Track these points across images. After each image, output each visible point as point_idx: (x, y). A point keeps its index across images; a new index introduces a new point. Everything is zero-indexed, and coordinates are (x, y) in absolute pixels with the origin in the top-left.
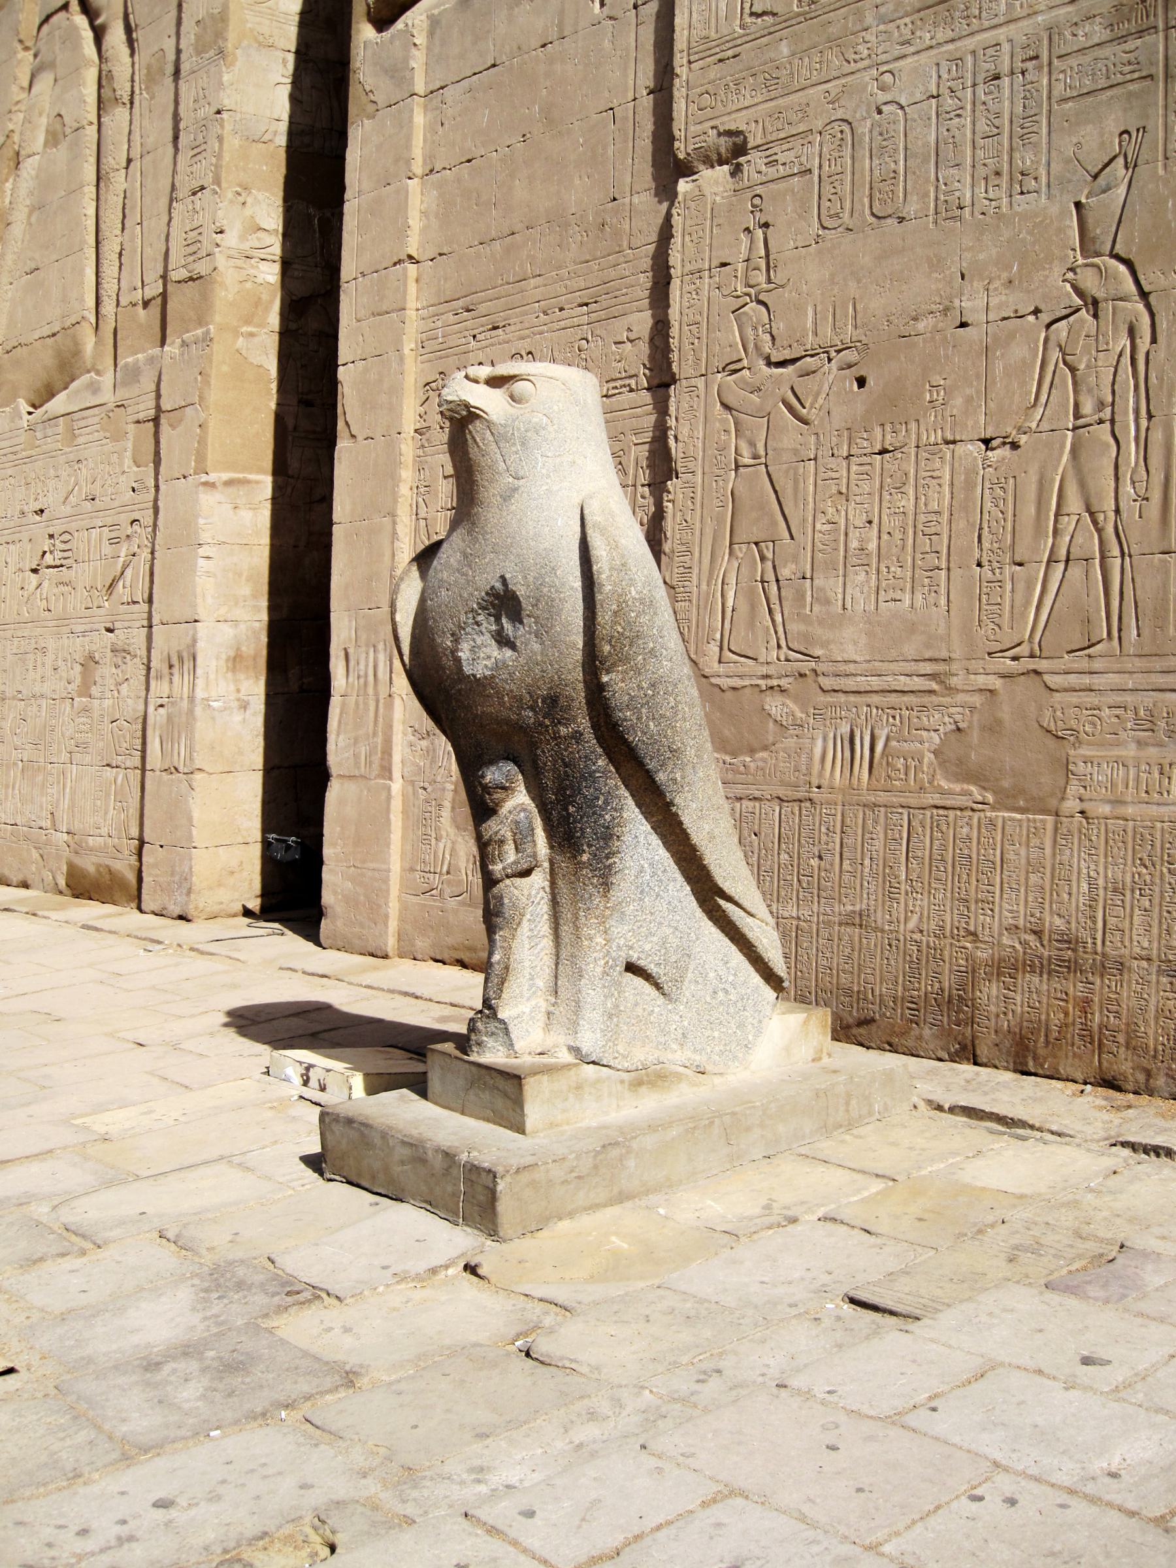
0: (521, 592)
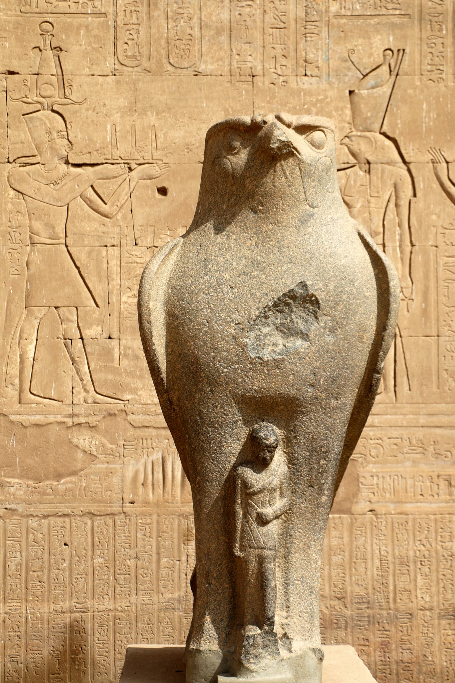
0: (321, 296)
